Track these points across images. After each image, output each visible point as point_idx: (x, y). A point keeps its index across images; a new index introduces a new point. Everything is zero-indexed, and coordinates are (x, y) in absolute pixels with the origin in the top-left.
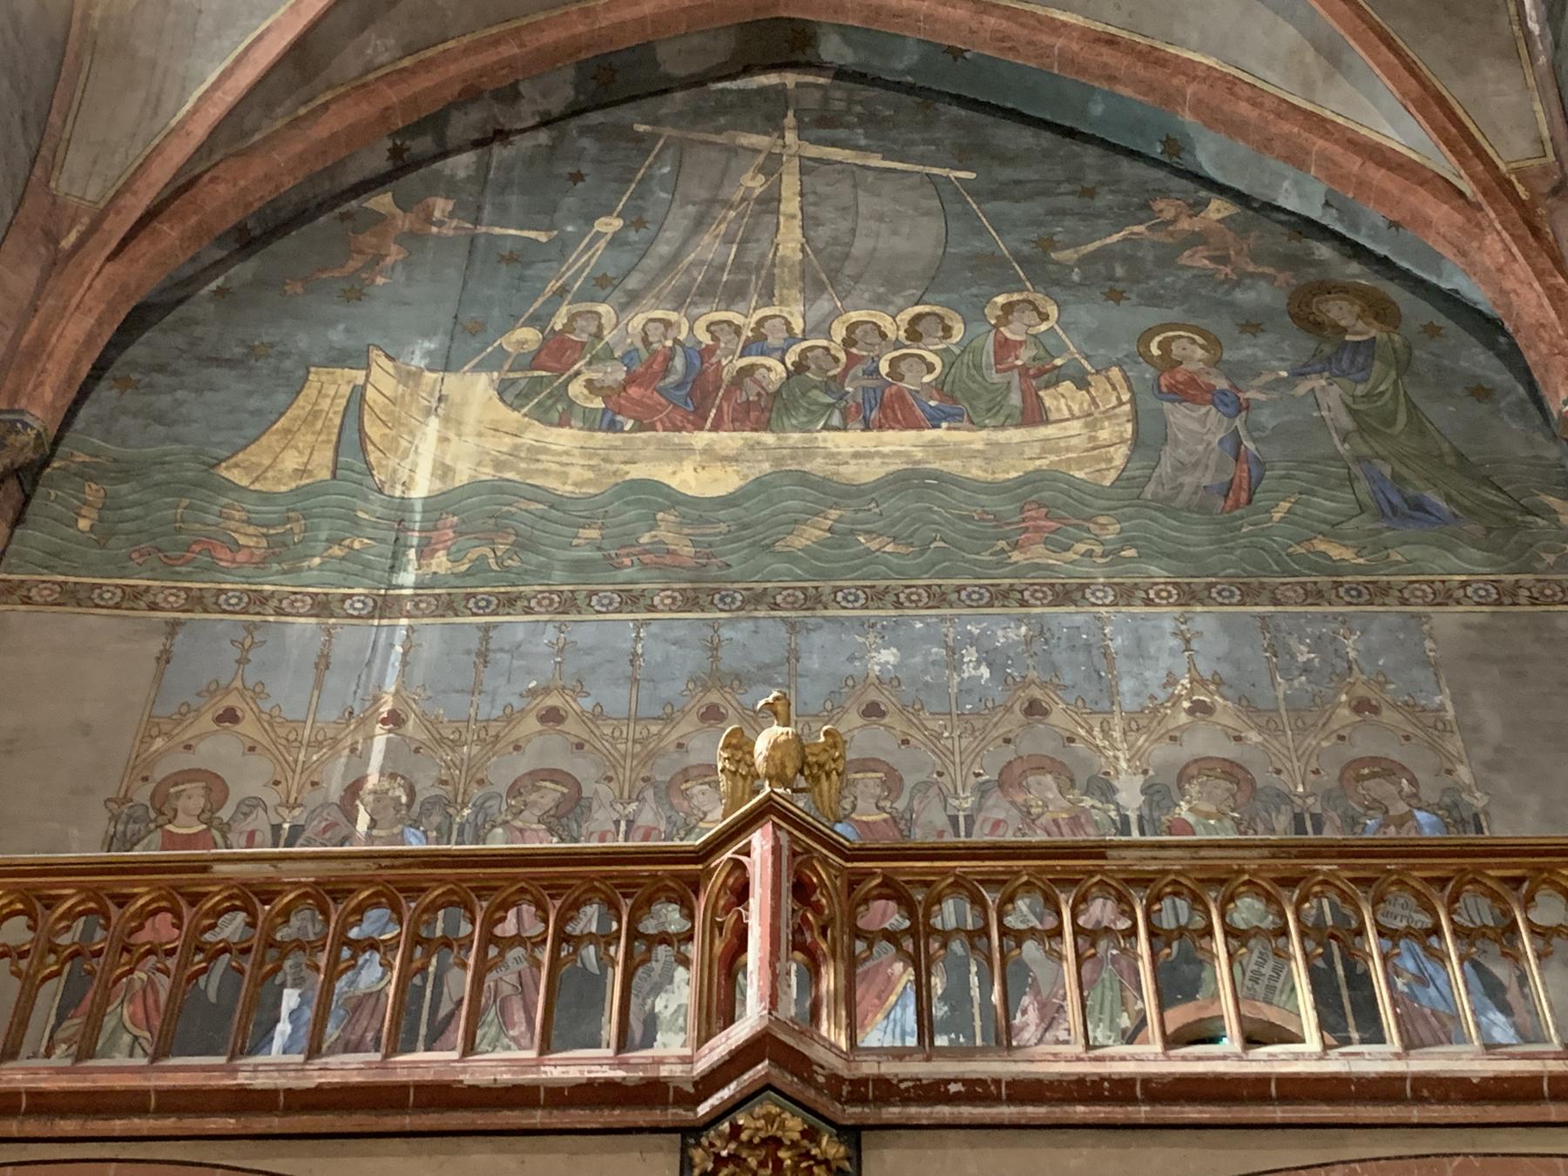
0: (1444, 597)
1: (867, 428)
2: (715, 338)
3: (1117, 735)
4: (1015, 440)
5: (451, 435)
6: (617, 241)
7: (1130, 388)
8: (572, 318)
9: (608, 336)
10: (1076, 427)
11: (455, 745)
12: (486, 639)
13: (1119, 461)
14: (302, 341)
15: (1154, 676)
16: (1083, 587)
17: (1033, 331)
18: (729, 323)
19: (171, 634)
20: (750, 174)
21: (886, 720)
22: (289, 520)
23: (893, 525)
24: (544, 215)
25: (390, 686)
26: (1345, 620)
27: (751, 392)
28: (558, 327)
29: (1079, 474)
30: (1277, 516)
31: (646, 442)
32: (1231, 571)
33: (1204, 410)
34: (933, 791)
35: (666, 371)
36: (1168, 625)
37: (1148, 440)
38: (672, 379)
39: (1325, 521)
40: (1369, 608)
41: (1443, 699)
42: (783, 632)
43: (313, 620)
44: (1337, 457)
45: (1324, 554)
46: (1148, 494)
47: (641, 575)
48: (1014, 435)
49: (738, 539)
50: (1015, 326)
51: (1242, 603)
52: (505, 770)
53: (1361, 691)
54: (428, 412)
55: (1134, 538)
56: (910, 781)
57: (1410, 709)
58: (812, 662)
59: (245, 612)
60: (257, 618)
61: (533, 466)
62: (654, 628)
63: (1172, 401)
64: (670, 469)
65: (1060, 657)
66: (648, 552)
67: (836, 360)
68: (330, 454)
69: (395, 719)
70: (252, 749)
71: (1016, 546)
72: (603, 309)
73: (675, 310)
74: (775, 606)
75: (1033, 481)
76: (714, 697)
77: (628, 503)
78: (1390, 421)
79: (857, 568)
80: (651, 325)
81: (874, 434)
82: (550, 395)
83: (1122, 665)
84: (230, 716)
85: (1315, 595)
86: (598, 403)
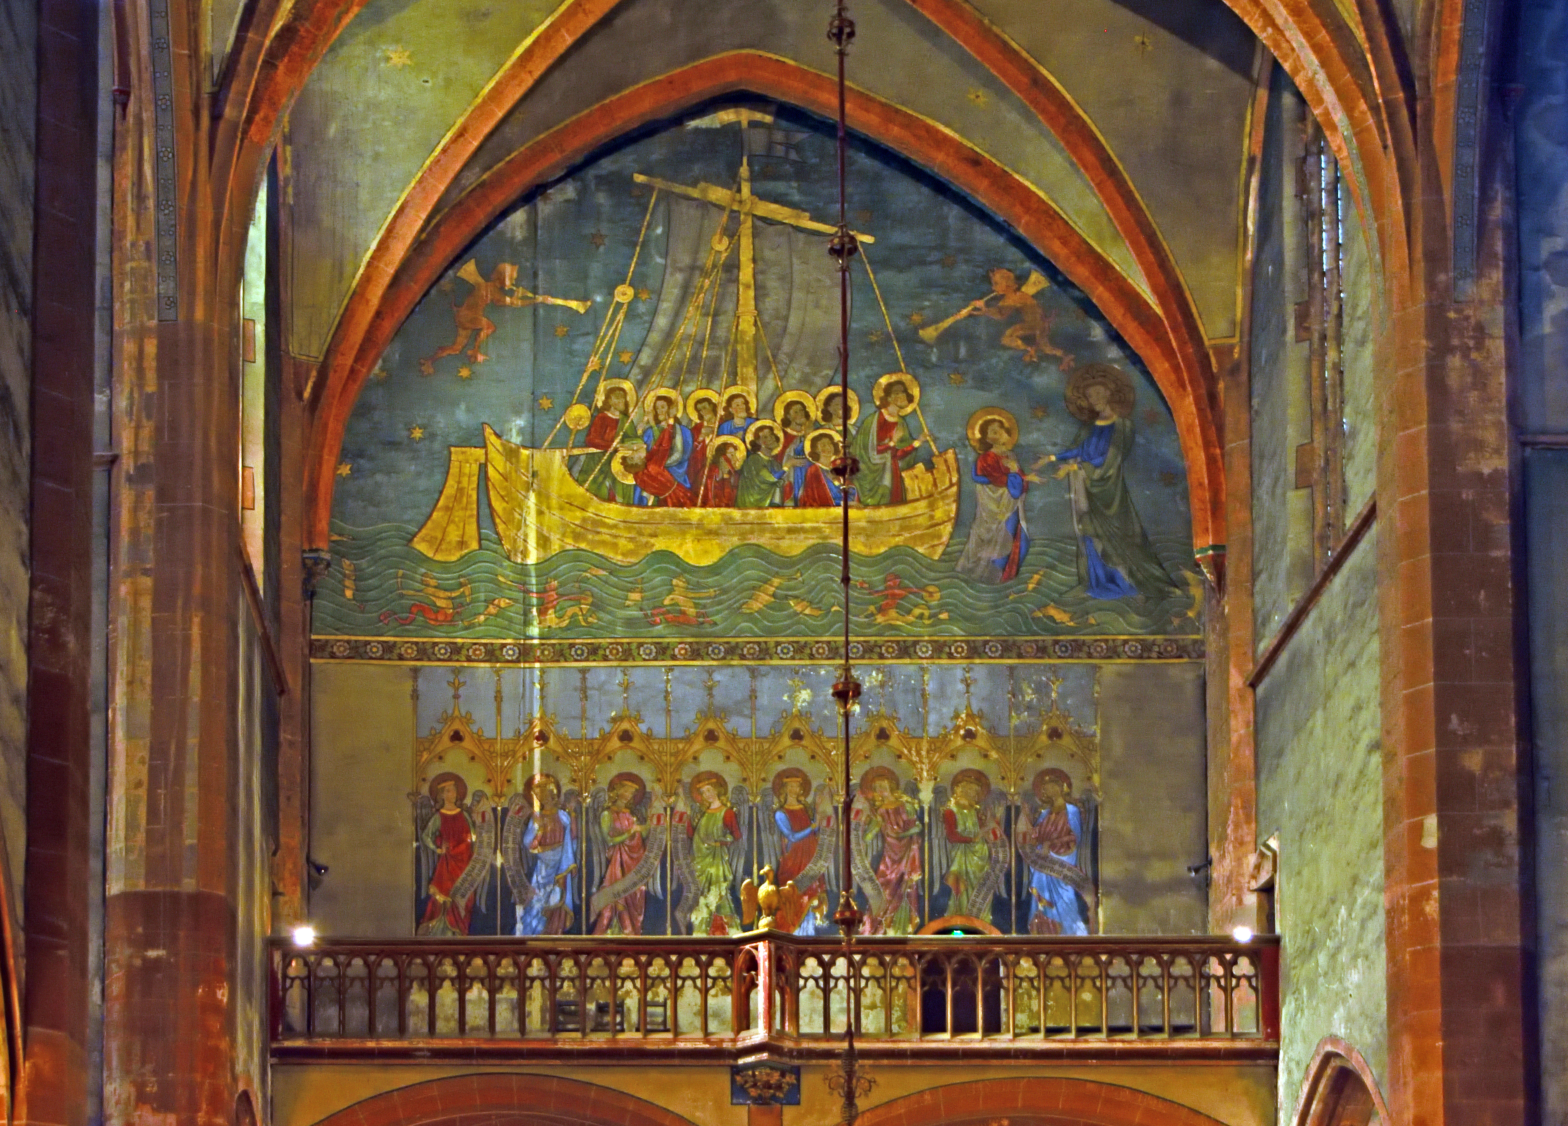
0: (1113, 652)
1: (796, 506)
2: (701, 417)
3: (924, 753)
4: (886, 518)
5: (544, 508)
6: (631, 314)
7: (958, 471)
8: (609, 393)
9: (634, 415)
10: (923, 504)
11: (576, 756)
12: (584, 679)
13: (945, 539)
15: (947, 711)
16: (915, 643)
17: (903, 413)
18: (707, 400)
19: (415, 679)
20: (717, 237)
21: (804, 742)
22: (461, 585)
23: (810, 592)
25: (537, 715)
26: (1054, 669)
27: (724, 472)
28: (600, 404)
29: (921, 550)
30: (1031, 586)
31: (663, 517)
32: (999, 631)
33: (1001, 491)
34: (826, 791)
35: (671, 450)
36: (959, 673)
38: (676, 456)
39: (1056, 591)
40: (1070, 661)
41: (1096, 729)
42: (747, 677)
43: (487, 665)
44: (1073, 538)
45: (1051, 618)
46: (959, 569)
47: (665, 632)
48: (884, 513)
49: (720, 603)
50: (892, 408)
51: (1001, 657)
52: (606, 773)
53: (1054, 723)
54: (528, 487)
55: (948, 604)
56: (815, 784)
57: (1079, 736)
58: (764, 700)
59: (449, 660)
60: (457, 664)
61: (597, 538)
62: (676, 672)
63: (982, 483)
64: (678, 542)
65: (900, 697)
66: (669, 612)
67: (777, 439)
68: (475, 526)
69: (543, 737)
70: (473, 758)
71: (881, 610)
72: (627, 385)
73: (674, 387)
74: (743, 657)
76: (711, 725)
77: (655, 571)
78: (1108, 506)
79: (789, 627)
80: (660, 403)
81: (798, 511)
82: (601, 471)
83: (931, 703)
84: (457, 737)
85: (1042, 651)
86: (630, 481)
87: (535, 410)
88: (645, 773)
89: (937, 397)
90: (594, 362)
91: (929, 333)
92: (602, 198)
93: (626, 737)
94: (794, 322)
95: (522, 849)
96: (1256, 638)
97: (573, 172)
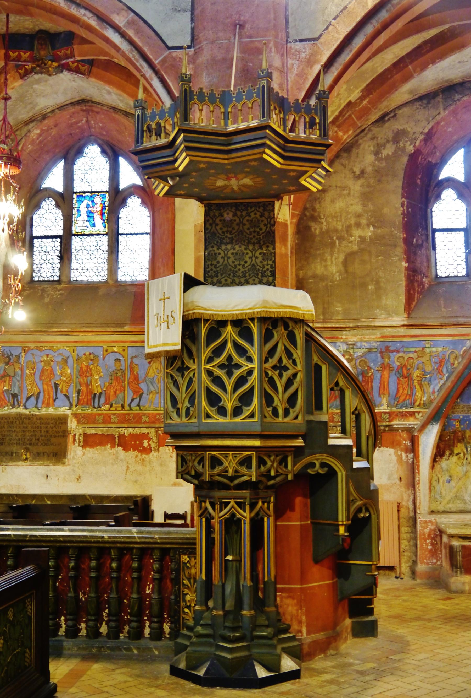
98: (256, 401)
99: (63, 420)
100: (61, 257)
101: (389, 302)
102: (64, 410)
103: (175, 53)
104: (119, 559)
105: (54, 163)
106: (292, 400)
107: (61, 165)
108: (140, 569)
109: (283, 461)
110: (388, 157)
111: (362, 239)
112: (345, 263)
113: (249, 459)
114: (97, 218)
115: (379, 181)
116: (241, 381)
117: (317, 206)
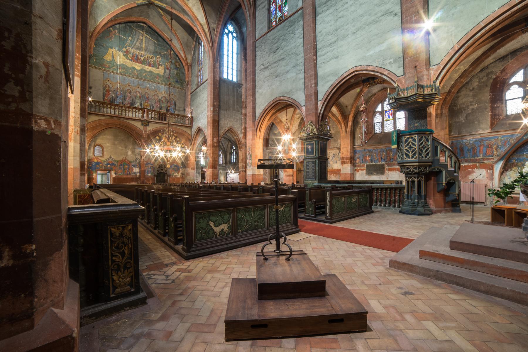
0: (178, 88)
6: (131, 41)
14: (107, 45)
24: (125, 35)
37: (165, 72)
48: (157, 69)
52: (126, 89)
69: (119, 83)
75: (158, 74)
87: (119, 47)
88: (131, 89)
89: (163, 60)
90: (126, 44)
91: (162, 53)
92: (128, 27)
93: (129, 85)
94: (149, 48)
95: (116, 95)
96: (191, 90)
97: (124, 23)
98: (417, 155)
99: (383, 165)
100: (382, 127)
101: (483, 126)
102: (384, 163)
103: (399, 78)
104: (390, 191)
105: (379, 104)
106: (428, 154)
107: (380, 105)
108: (395, 193)
109: (426, 168)
110: (484, 82)
111: (473, 109)
112: (466, 117)
113: (416, 167)
114: (391, 116)
115: (480, 90)
116: (413, 150)
117: (456, 102)
